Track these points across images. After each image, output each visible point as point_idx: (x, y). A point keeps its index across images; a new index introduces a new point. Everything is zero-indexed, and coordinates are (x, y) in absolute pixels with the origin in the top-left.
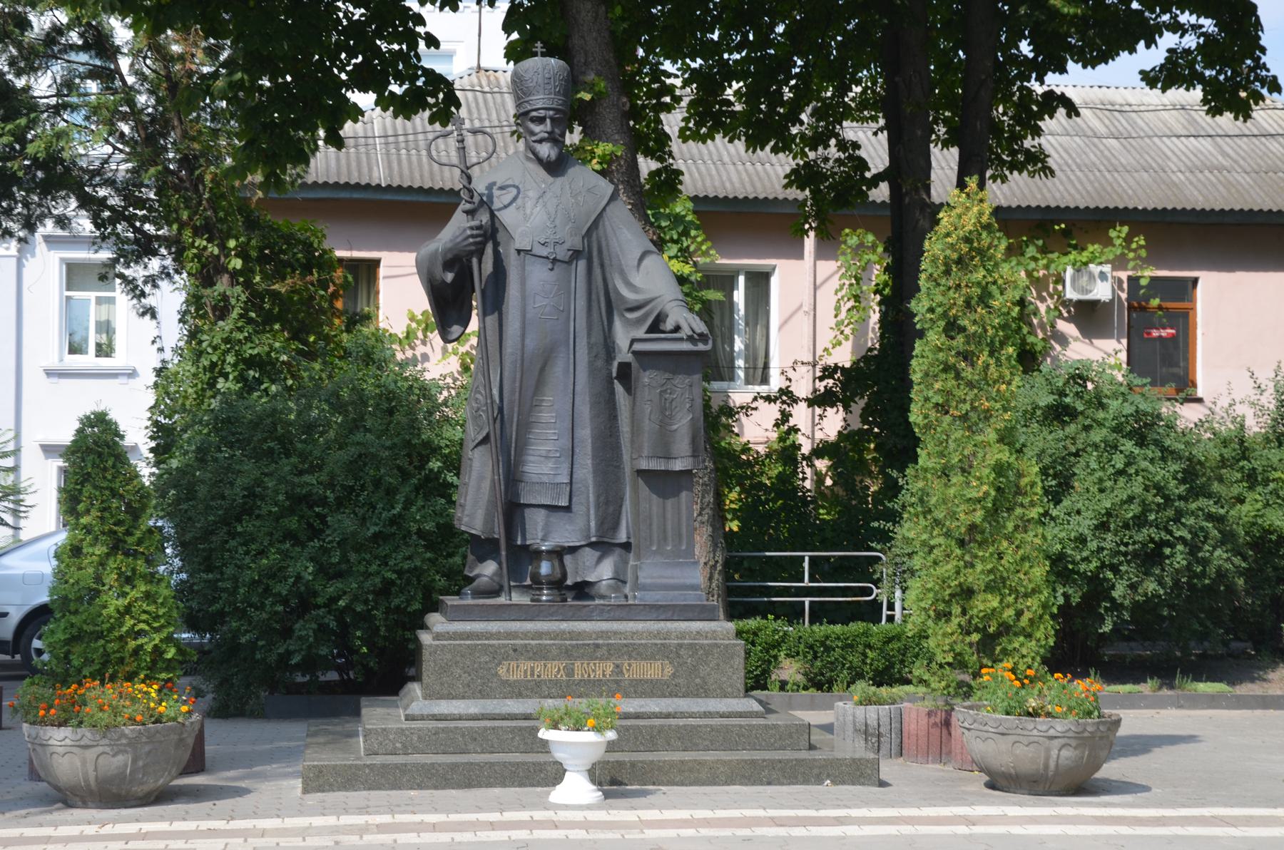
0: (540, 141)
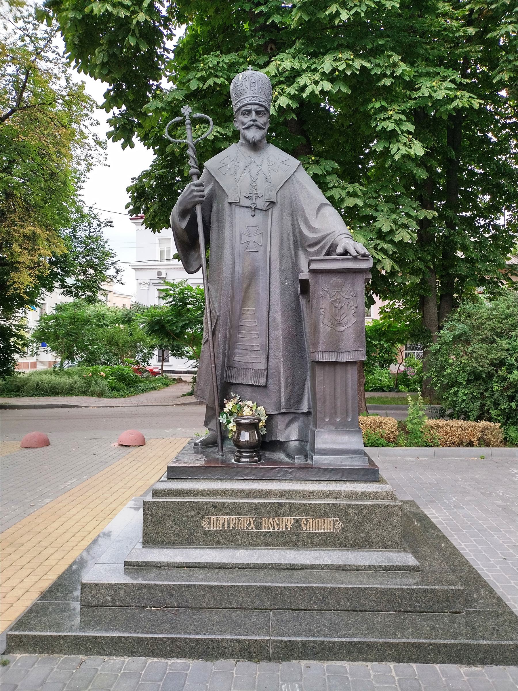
0: (248, 128)
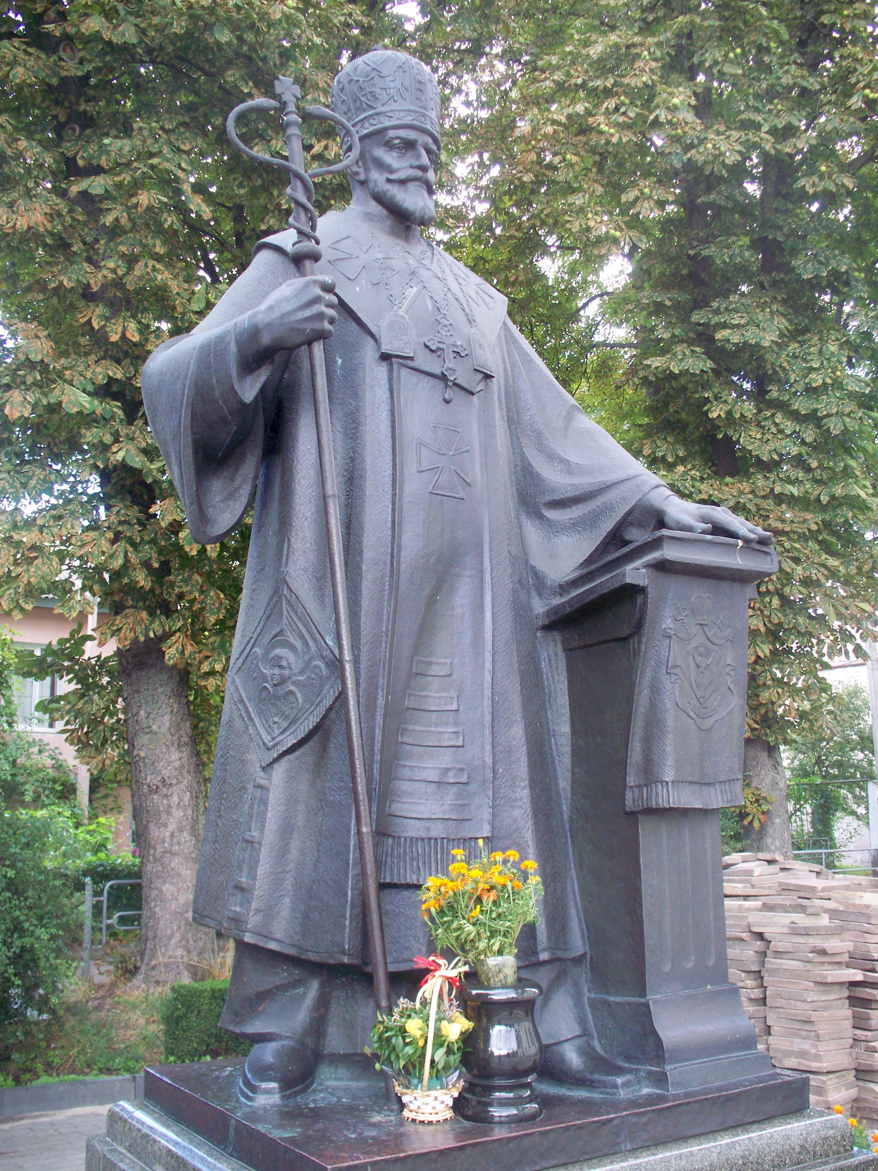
0: (403, 182)
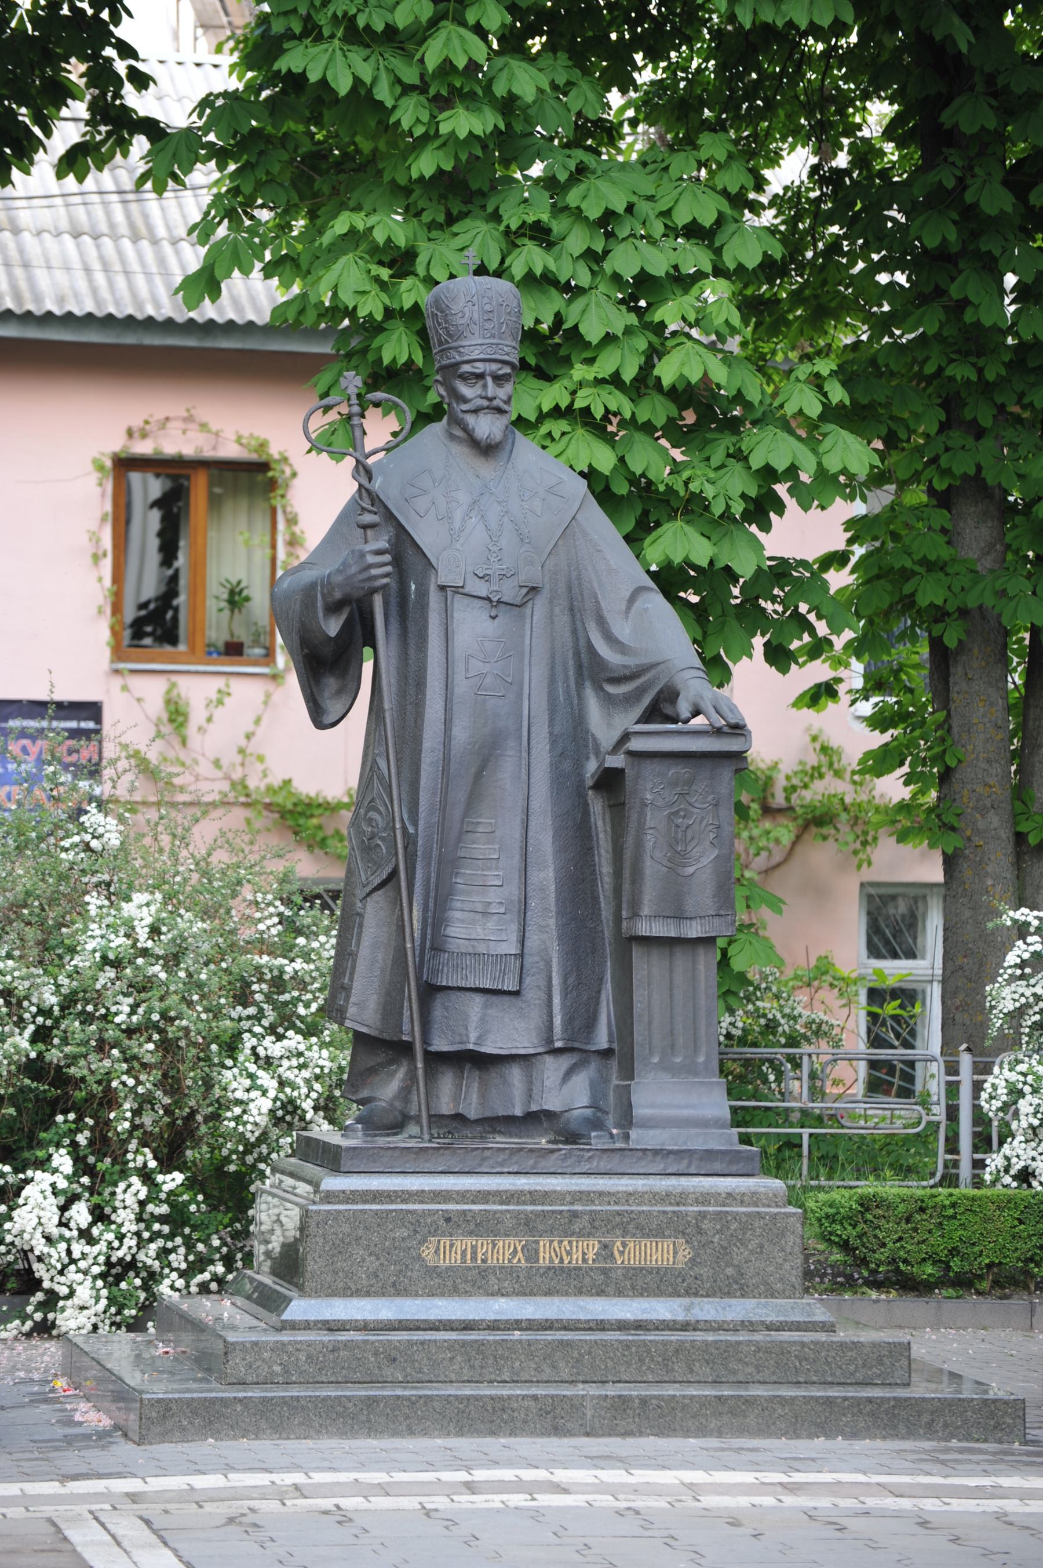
0: (476, 411)
